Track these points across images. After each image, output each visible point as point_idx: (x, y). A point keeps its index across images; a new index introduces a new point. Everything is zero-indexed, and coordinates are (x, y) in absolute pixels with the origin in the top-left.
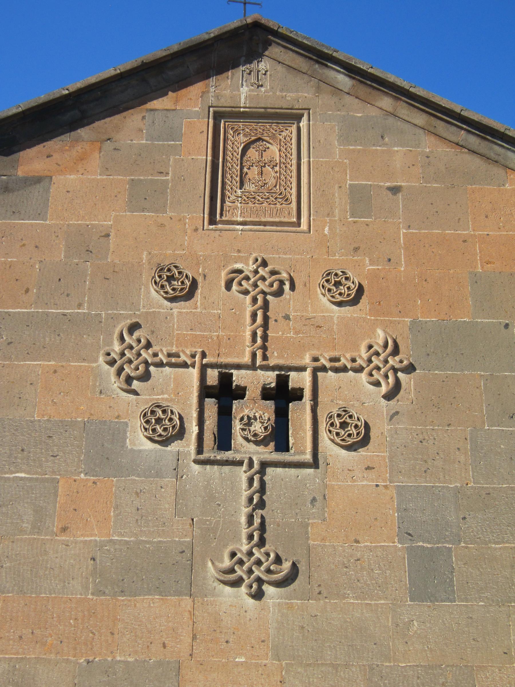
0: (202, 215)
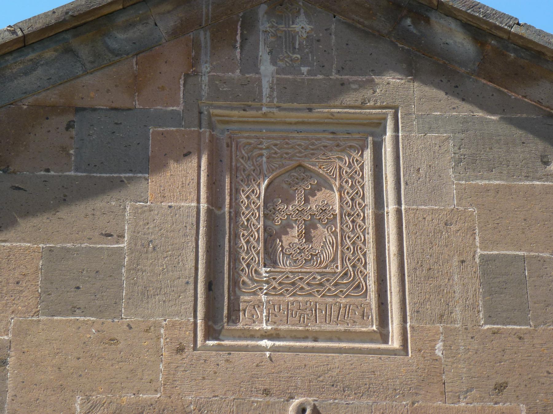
0: (192, 320)
